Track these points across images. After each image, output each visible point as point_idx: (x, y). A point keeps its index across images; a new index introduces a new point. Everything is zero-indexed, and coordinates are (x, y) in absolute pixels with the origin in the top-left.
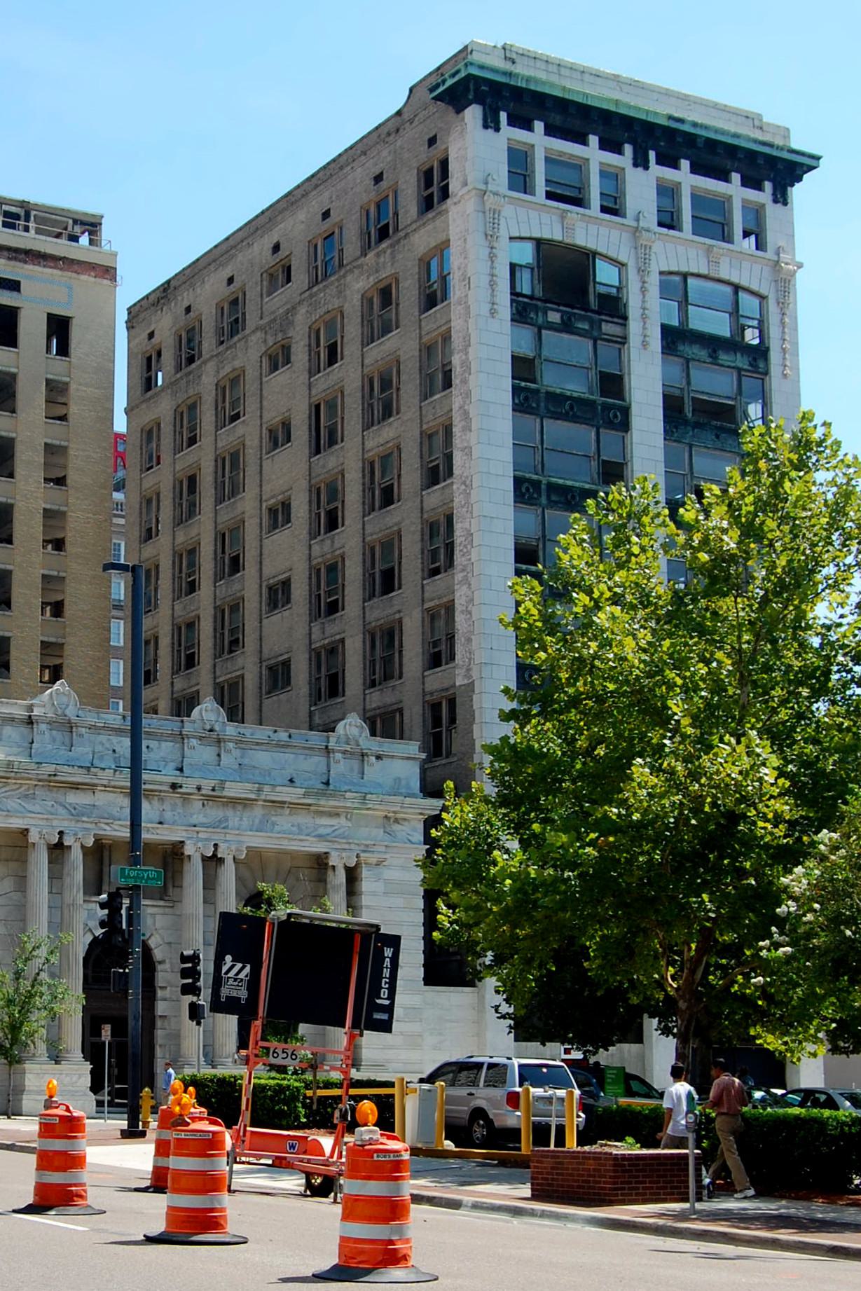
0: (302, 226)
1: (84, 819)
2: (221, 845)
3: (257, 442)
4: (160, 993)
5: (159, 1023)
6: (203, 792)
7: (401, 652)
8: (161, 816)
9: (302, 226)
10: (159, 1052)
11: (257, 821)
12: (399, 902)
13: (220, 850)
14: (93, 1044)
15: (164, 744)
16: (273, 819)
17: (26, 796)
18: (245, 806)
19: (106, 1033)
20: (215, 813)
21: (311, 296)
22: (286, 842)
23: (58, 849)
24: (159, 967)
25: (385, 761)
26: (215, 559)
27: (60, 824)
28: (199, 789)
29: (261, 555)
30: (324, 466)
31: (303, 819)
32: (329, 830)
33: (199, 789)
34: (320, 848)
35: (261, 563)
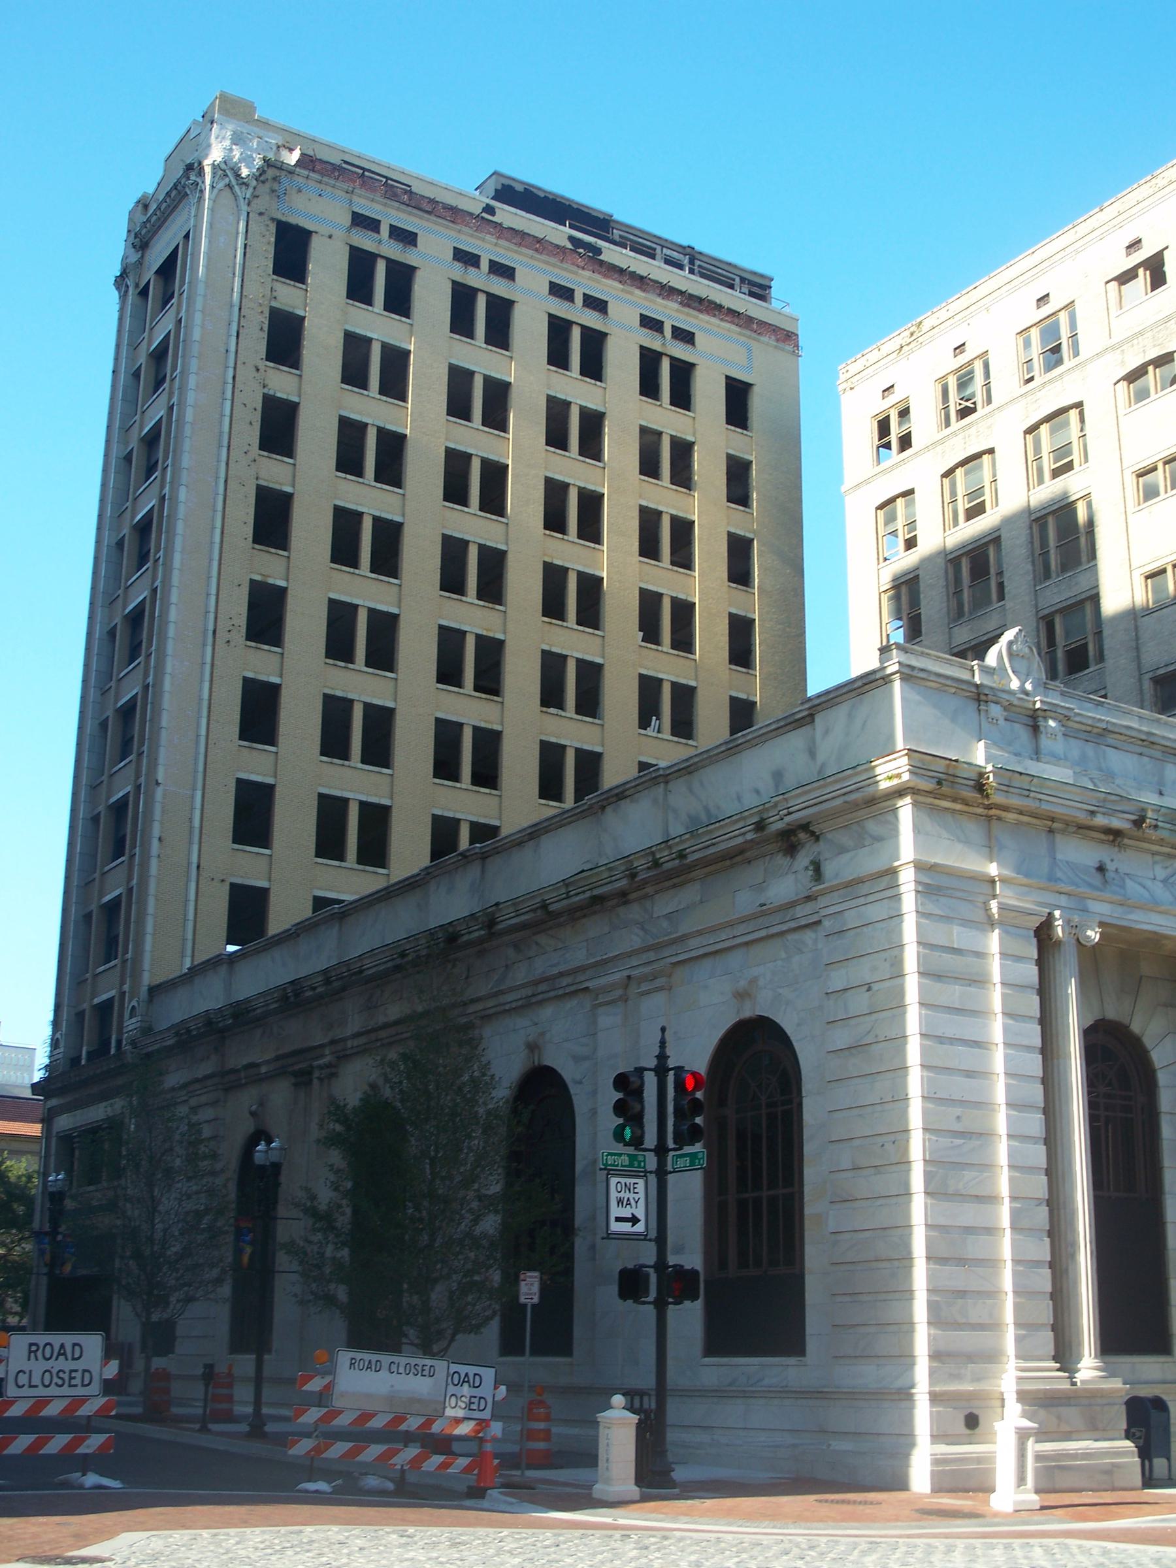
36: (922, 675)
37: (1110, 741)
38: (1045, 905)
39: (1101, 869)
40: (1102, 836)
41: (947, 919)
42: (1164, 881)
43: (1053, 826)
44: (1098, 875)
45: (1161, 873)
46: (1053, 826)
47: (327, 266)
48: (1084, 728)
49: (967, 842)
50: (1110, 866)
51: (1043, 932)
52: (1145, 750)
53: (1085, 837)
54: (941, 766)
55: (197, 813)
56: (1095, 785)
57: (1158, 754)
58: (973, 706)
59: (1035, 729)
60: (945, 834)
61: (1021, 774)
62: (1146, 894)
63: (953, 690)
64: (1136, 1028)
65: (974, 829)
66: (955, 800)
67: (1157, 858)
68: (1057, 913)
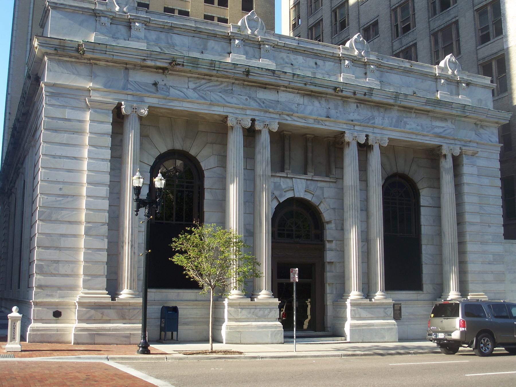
1: (271, 110)
2: (370, 134)
4: (328, 245)
5: (328, 267)
6: (358, 96)
7: (458, 41)
10: (328, 289)
11: (394, 120)
12: (486, 181)
13: (370, 138)
14: (280, 285)
15: (327, 63)
16: (405, 120)
17: (226, 91)
18: (386, 109)
19: (295, 276)
20: (365, 113)
22: (414, 136)
24: (327, 226)
25: (472, 88)
26: (332, 25)
27: (251, 114)
28: (354, 93)
29: (359, 14)
31: (424, 121)
32: (441, 130)
33: (354, 93)
34: (435, 142)
35: (359, 18)
36: (61, 6)
37: (175, 32)
38: (116, 99)
39: (155, 84)
40: (155, 70)
41: (64, 107)
42: (194, 89)
43: (127, 67)
44: (154, 87)
46: (127, 67)
48: (159, 26)
49: (79, 74)
50: (161, 83)
52: (195, 35)
53: (147, 71)
54: (57, 42)
56: (161, 50)
57: (205, 37)
58: (93, 18)
59: (130, 28)
60: (66, 71)
61: (99, 44)
62: (182, 94)
63: (81, 12)
64: (192, 152)
65: (83, 69)
66: (71, 57)
67: (190, 79)
68: (123, 103)
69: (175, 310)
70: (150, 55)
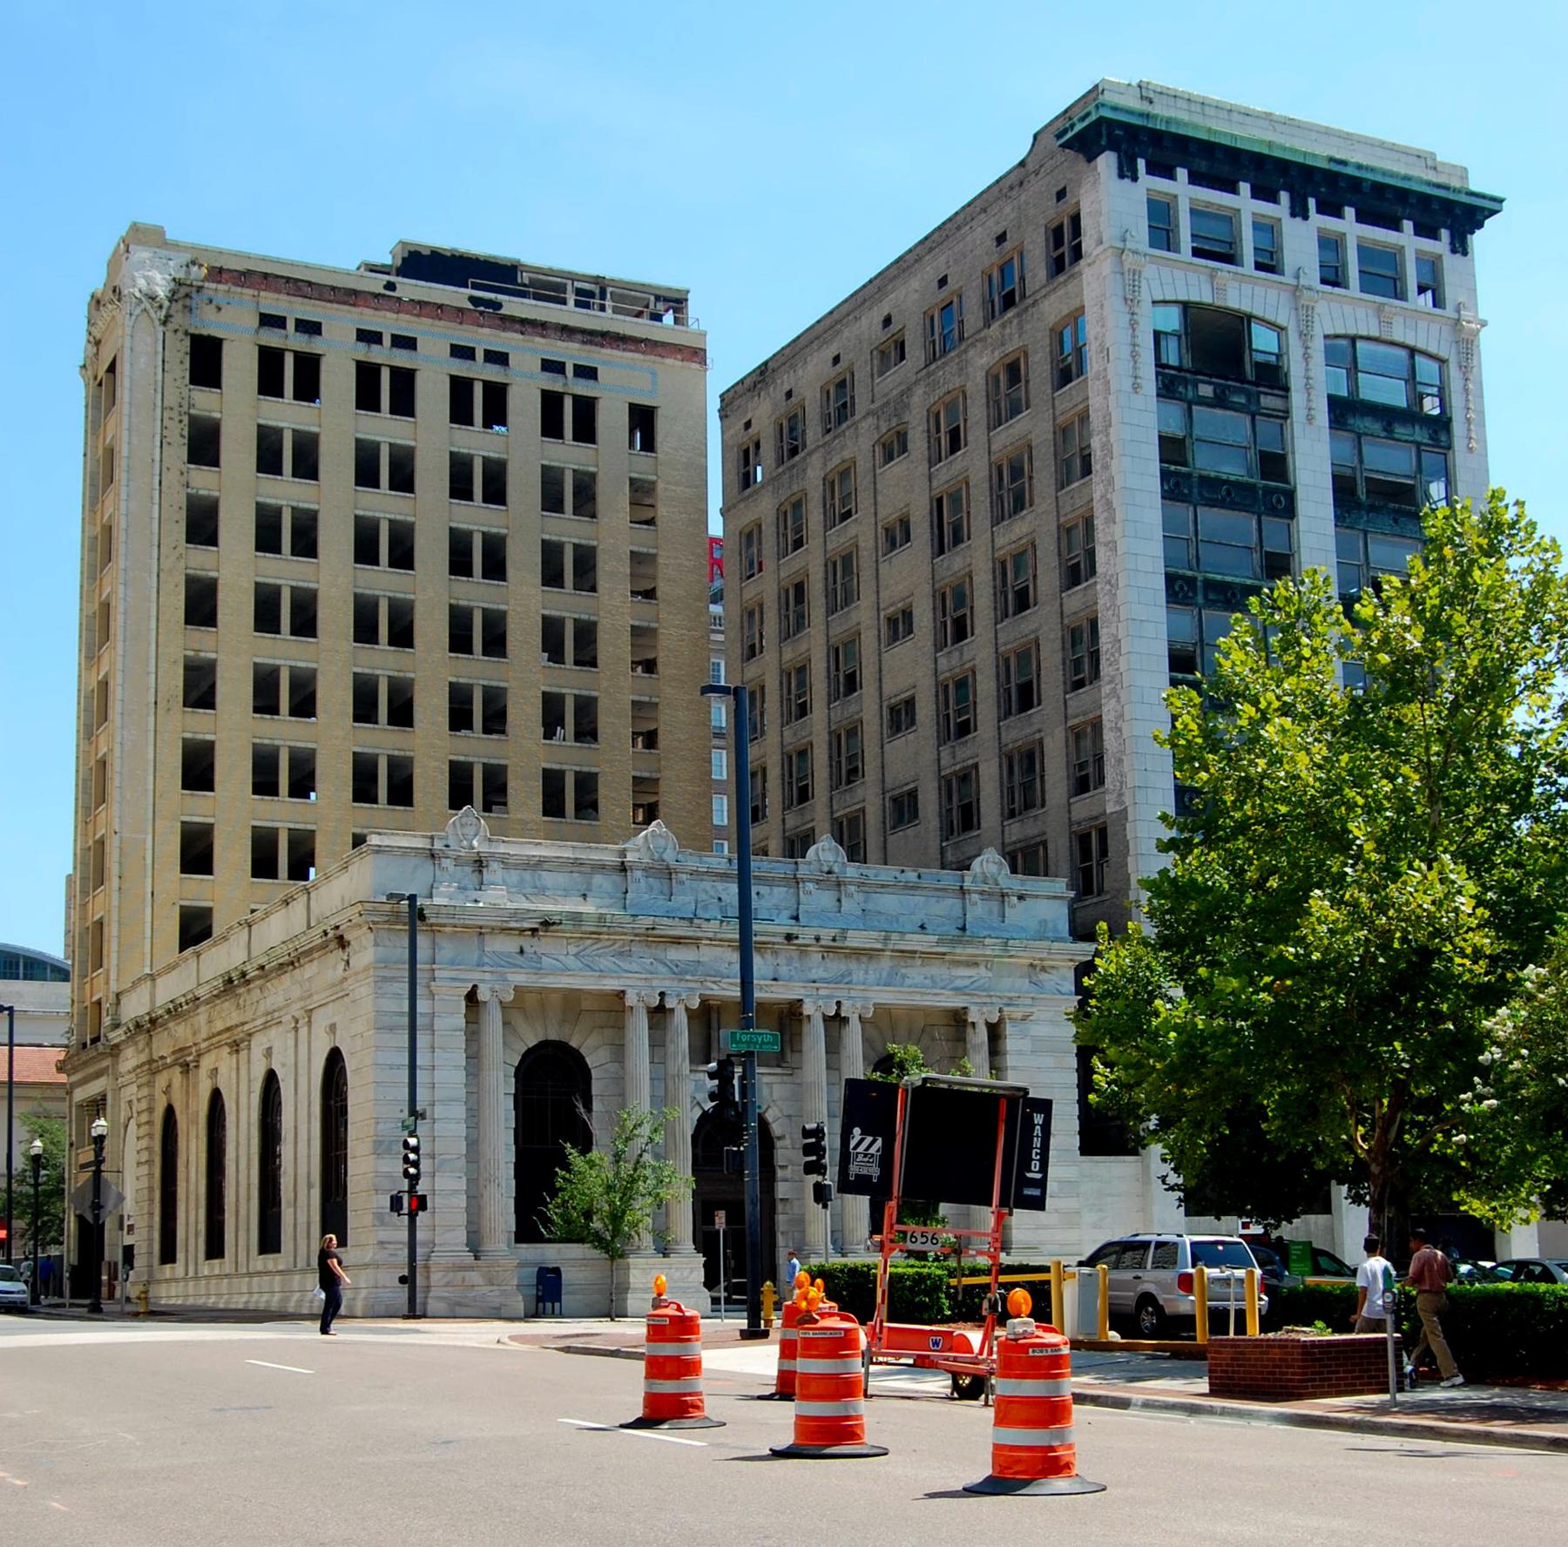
0: (916, 296)
3: (871, 543)
4: (780, 1173)
5: (780, 1207)
7: (1042, 777)
8: (776, 971)
9: (916, 296)
10: (780, 1240)
11: (884, 974)
12: (1049, 1061)
14: (706, 1234)
15: (776, 890)
17: (621, 953)
18: (871, 957)
20: (836, 966)
21: (929, 375)
22: (918, 997)
23: (659, 1013)
24: (778, 1144)
25: (1029, 902)
27: (660, 984)
28: (818, 939)
29: (880, 670)
30: (948, 568)
31: (938, 970)
32: (967, 982)
33: (818, 939)
34: (957, 1002)
45: (573, 950)
47: (239, 365)
51: (471, 997)
55: (149, 853)
64: (573, 1044)
69: (557, 1271)
70: (515, 914)
